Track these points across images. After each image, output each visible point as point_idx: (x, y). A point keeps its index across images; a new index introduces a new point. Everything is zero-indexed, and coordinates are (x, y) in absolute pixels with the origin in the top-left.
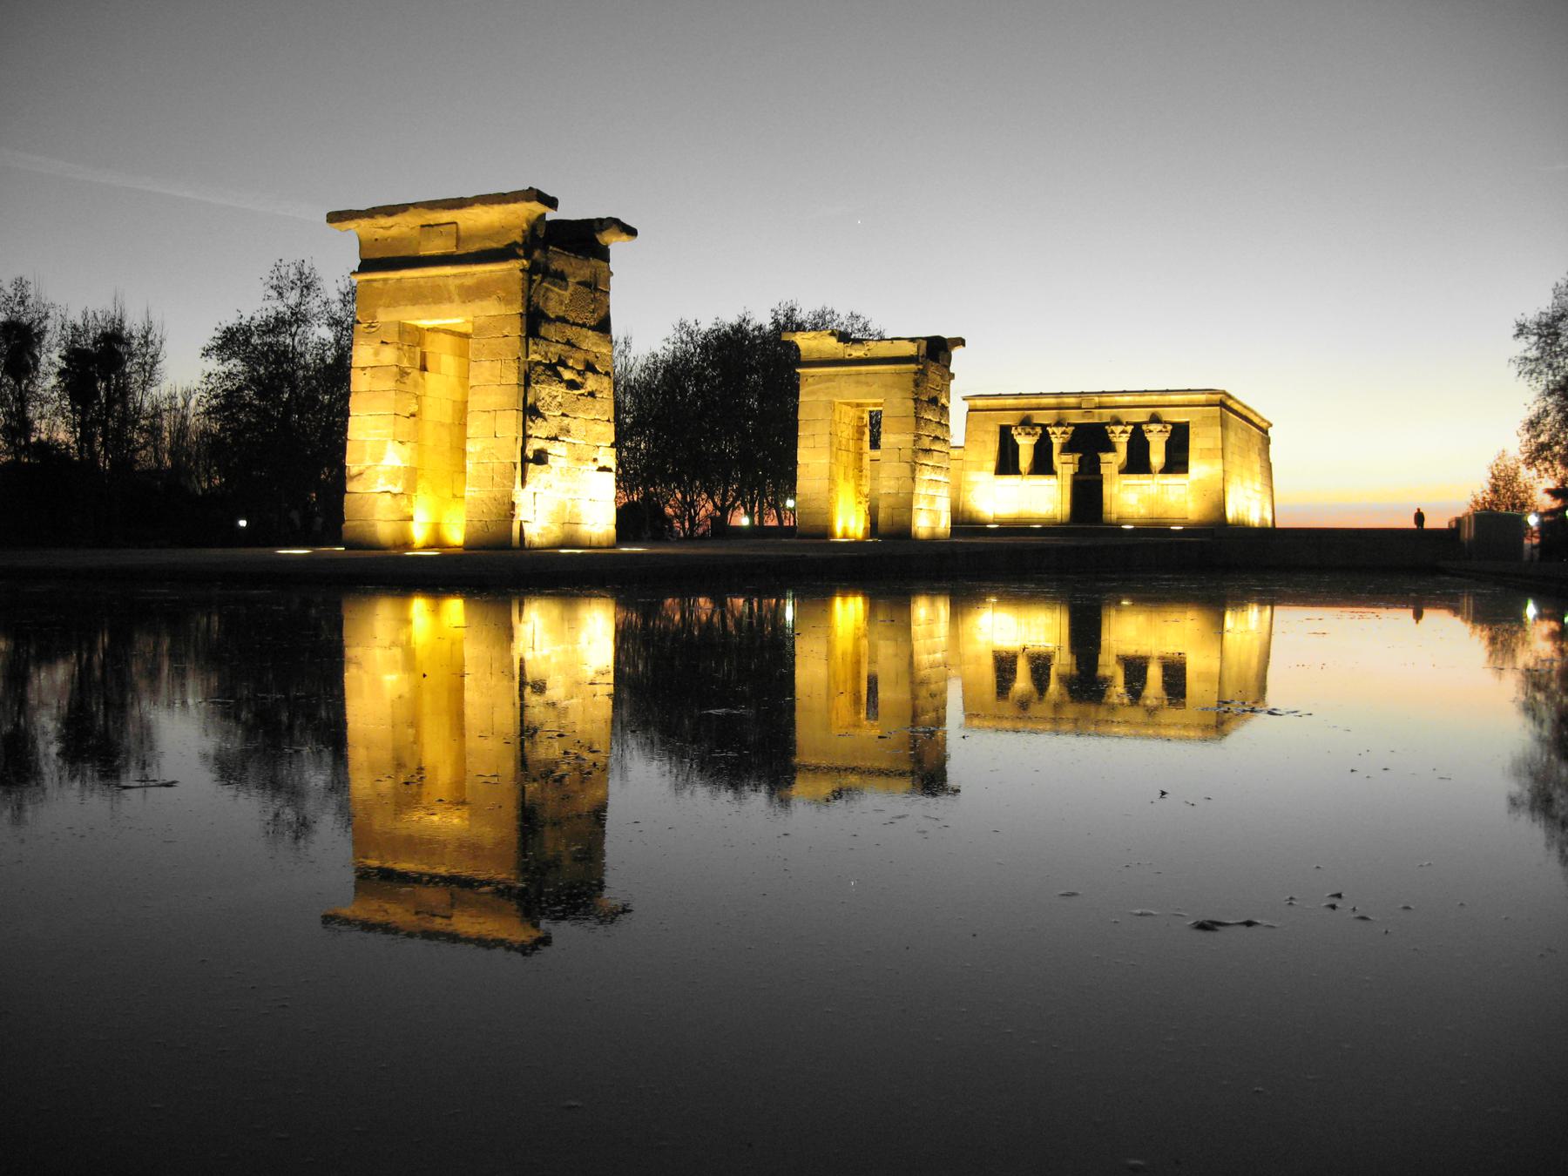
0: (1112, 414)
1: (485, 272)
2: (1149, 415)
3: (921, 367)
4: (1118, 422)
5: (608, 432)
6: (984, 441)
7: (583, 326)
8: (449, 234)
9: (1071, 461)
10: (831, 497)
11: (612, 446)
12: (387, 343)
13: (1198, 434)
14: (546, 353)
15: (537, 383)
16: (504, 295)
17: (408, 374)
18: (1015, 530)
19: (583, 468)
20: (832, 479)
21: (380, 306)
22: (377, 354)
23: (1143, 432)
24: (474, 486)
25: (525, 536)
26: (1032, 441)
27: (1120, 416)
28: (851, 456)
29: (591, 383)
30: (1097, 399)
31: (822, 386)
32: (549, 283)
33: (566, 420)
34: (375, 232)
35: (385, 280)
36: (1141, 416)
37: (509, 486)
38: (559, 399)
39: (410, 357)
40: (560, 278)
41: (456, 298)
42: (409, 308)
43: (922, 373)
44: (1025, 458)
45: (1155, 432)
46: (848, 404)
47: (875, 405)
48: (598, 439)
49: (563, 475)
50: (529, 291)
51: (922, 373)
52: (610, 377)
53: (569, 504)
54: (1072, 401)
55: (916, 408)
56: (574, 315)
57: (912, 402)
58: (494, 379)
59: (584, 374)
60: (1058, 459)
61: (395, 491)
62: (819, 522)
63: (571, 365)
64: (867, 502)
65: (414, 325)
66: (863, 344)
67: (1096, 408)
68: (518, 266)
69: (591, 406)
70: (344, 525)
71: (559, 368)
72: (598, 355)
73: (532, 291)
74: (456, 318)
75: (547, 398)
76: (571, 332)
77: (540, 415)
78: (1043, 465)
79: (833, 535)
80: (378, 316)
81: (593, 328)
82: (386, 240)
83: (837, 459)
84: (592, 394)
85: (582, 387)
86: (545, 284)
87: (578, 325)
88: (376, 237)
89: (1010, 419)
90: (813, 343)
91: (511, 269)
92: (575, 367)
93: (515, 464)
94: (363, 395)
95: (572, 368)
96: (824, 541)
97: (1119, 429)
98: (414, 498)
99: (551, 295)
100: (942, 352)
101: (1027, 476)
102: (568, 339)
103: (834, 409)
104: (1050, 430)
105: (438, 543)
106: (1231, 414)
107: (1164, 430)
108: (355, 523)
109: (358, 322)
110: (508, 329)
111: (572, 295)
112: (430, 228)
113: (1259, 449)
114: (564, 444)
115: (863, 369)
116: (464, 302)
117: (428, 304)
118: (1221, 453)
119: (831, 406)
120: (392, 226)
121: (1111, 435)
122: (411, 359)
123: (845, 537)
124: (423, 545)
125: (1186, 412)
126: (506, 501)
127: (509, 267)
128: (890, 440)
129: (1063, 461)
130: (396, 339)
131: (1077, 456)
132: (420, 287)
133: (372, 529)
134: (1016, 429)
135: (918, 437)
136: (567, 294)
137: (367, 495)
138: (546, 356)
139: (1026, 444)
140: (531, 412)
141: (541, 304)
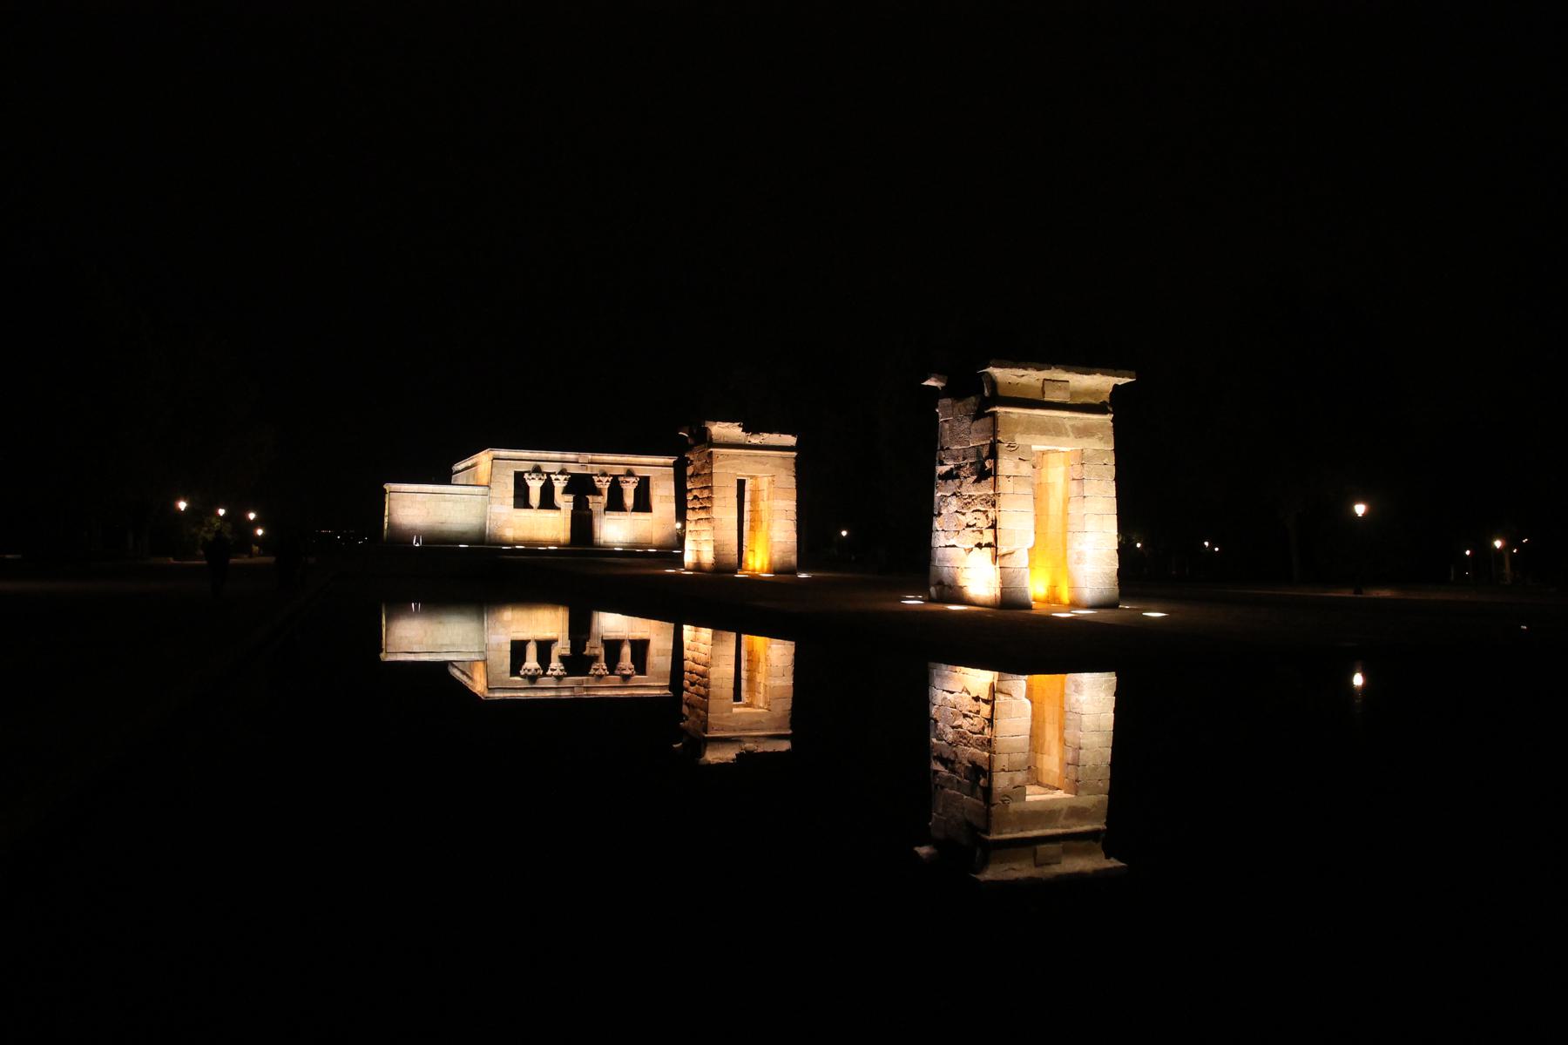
1: (1089, 419)
4: (604, 475)
6: (506, 483)
22: (1017, 466)
26: (541, 483)
27: (606, 470)
30: (590, 457)
35: (1018, 413)
36: (620, 470)
44: (535, 497)
67: (589, 463)
74: (1068, 446)
78: (547, 502)
89: (524, 467)
94: (1010, 496)
97: (606, 479)
104: (553, 477)
116: (1076, 438)
117: (1052, 435)
120: (1023, 376)
132: (1046, 423)
134: (530, 475)
139: (535, 485)
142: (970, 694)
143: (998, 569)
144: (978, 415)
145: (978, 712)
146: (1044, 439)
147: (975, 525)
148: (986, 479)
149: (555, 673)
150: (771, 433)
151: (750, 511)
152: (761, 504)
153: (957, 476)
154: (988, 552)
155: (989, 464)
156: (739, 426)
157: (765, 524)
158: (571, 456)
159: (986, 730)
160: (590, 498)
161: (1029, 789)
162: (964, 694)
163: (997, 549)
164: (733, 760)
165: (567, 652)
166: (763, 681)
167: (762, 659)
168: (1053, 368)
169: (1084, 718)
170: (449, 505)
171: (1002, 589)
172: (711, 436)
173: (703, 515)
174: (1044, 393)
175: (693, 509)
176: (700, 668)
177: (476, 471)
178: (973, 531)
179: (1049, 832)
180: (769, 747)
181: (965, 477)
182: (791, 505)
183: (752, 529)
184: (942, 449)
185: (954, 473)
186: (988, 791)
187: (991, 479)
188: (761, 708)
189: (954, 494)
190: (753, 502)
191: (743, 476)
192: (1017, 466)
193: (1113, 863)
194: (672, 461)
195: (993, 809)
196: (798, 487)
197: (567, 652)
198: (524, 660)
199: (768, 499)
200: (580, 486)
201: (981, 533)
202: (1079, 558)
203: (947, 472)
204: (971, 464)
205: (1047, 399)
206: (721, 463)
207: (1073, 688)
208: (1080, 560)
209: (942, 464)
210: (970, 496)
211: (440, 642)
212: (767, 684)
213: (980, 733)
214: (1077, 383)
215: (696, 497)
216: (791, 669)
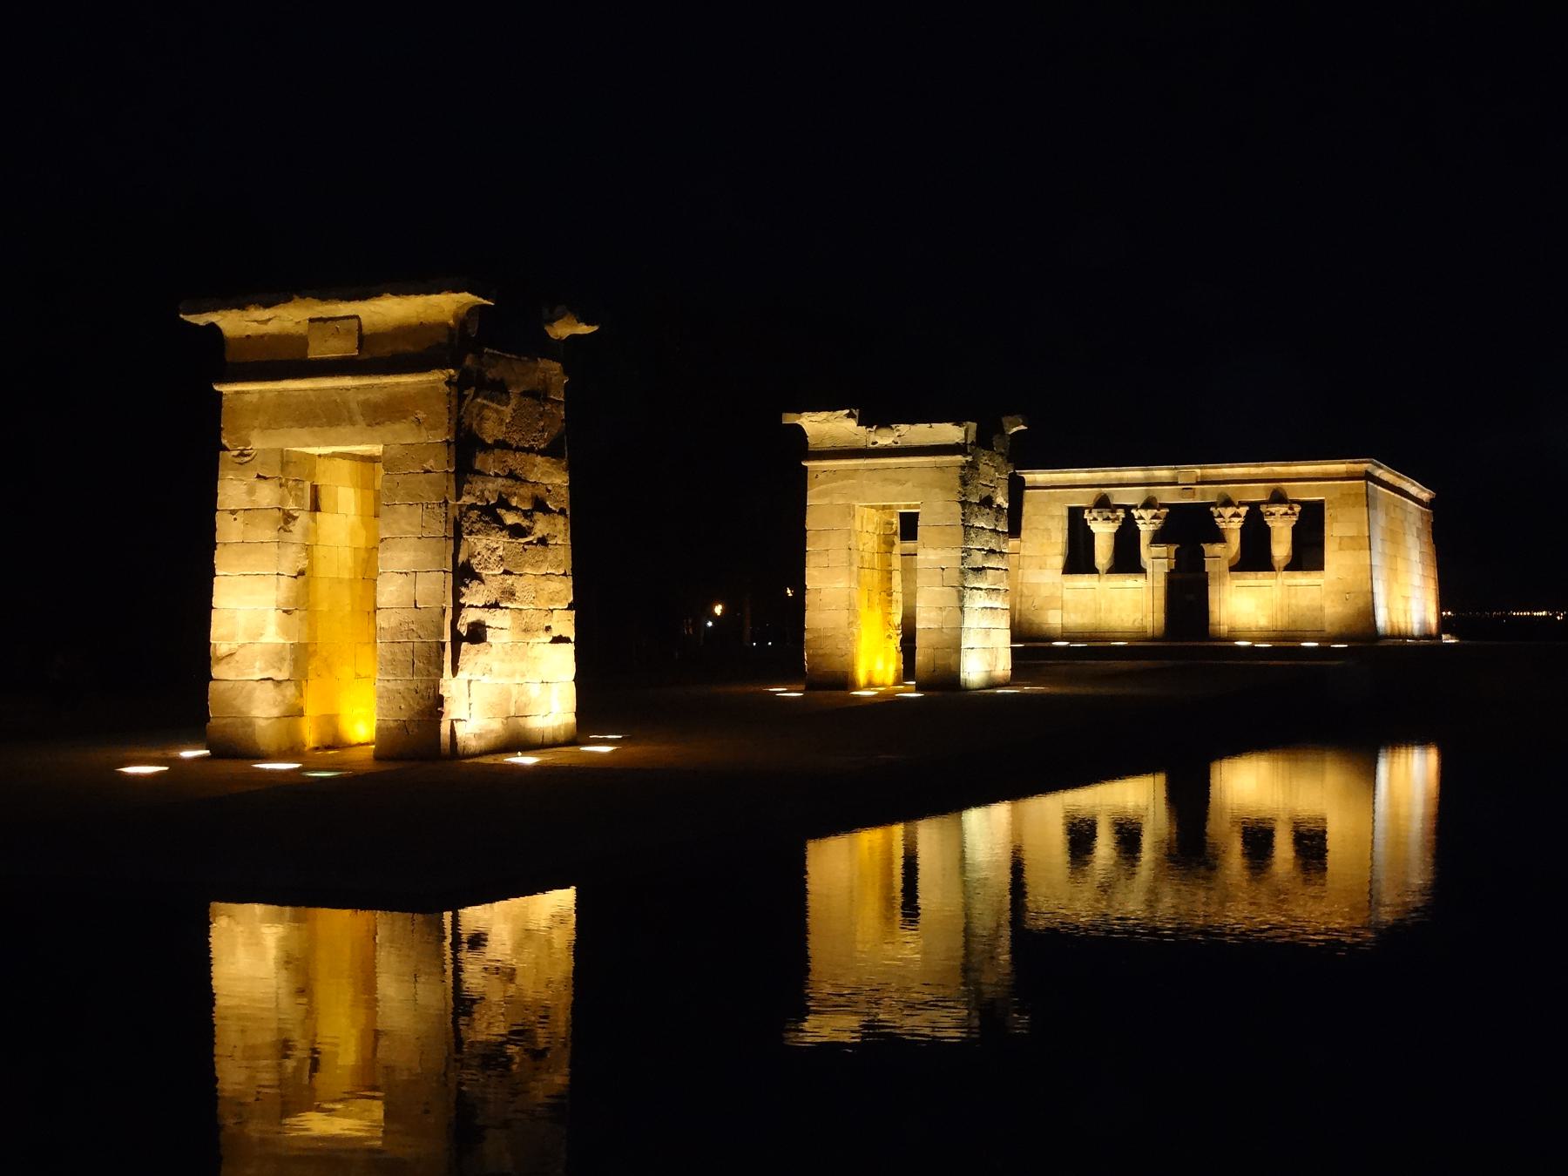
0: (1220, 491)
2: (1270, 493)
3: (969, 458)
4: (1228, 503)
5: (564, 589)
6: (1047, 530)
7: (530, 450)
8: (349, 332)
9: (1165, 555)
10: (853, 634)
11: (570, 607)
12: (265, 478)
13: (1337, 518)
14: (482, 492)
15: (471, 533)
16: (424, 416)
17: (295, 518)
19: (531, 641)
20: (851, 609)
21: (255, 427)
22: (251, 491)
23: (1261, 515)
24: (387, 673)
25: (458, 740)
27: (1230, 496)
28: (877, 576)
29: (541, 527)
30: (1198, 471)
31: (840, 483)
32: (485, 398)
33: (510, 580)
34: (247, 326)
35: (260, 391)
36: (1258, 493)
37: (436, 675)
38: (500, 552)
39: (296, 495)
40: (498, 390)
41: (359, 418)
42: (296, 431)
43: (972, 466)
44: (1103, 552)
45: (1278, 515)
46: (872, 507)
47: (908, 507)
48: (551, 600)
49: (506, 653)
50: (460, 405)
51: (972, 466)
52: (566, 516)
53: (515, 691)
55: (964, 514)
56: (517, 437)
57: (959, 507)
58: (414, 530)
59: (532, 515)
60: (1147, 553)
61: (280, 677)
62: (836, 665)
63: (514, 504)
64: (898, 635)
65: (301, 452)
66: (892, 429)
67: (1198, 483)
68: (442, 377)
69: (542, 558)
70: (208, 724)
71: (498, 511)
72: (550, 488)
73: (462, 413)
75: (484, 552)
76: (514, 460)
77: (477, 577)
78: (1126, 560)
79: (855, 686)
80: (252, 442)
81: (542, 453)
82: (262, 337)
83: (859, 582)
84: (543, 541)
85: (530, 534)
86: (479, 400)
87: (519, 449)
88: (249, 333)
89: (1083, 498)
90: (826, 427)
91: (435, 381)
92: (520, 506)
93: (443, 645)
95: (516, 509)
96: (841, 693)
97: (1229, 511)
98: (304, 683)
99: (487, 413)
100: (998, 436)
101: (1106, 576)
102: (510, 470)
103: (854, 516)
104: (1136, 513)
105: (335, 743)
106: (1379, 488)
107: (1290, 512)
108: (224, 721)
109: (226, 449)
110: (431, 462)
111: (514, 411)
112: (322, 323)
113: (1418, 528)
114: (508, 611)
116: (369, 425)
118: (1367, 540)
119: (849, 512)
120: (270, 320)
121: (1218, 520)
122: (298, 499)
123: (870, 685)
124: (316, 746)
125: (1319, 488)
126: (431, 695)
127: (431, 378)
128: (932, 557)
129: (1154, 555)
130: (278, 473)
131: (1174, 548)
133: (250, 730)
134: (1090, 512)
135: (968, 551)
136: (508, 410)
137: (241, 684)
138: (482, 497)
139: (1103, 532)
140: (464, 574)
141: (474, 426)
146: (304, 433)
150: (912, 422)
156: (850, 416)
158: (1163, 473)
168: (296, 297)
174: (307, 345)
192: (251, 491)
205: (312, 355)
214: (376, 318)
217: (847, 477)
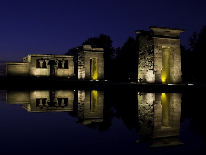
4: (57, 60)
6: (35, 62)
18: (41, 78)
22: (158, 51)
36: (61, 59)
42: (163, 44)
44: (41, 66)
54: (50, 56)
78: (44, 67)
89: (39, 58)
90: (87, 47)
97: (58, 61)
104: (45, 61)
109: (154, 45)
115: (95, 52)
125: (68, 59)
139: (41, 62)
142: (148, 104)
143: (154, 75)
144: (149, 39)
145: (150, 108)
146: (165, 45)
147: (149, 65)
148: (151, 54)
149: (46, 106)
150: (98, 47)
151: (93, 66)
152: (96, 64)
153: (144, 54)
154: (152, 70)
155: (152, 51)
156: (91, 46)
157: (96, 69)
158: (50, 56)
159: (152, 112)
160: (54, 65)
161: (162, 126)
162: (146, 104)
163: (154, 70)
164: (90, 124)
165: (49, 101)
166: (97, 105)
167: (96, 100)
169: (174, 109)
170: (22, 67)
171: (155, 79)
172: (84, 49)
173: (82, 67)
174: (164, 34)
175: (80, 66)
176: (82, 102)
177: (27, 60)
178: (148, 66)
179: (167, 136)
180: (98, 121)
181: (146, 54)
182: (102, 64)
183: (93, 70)
184: (140, 48)
185: (144, 53)
186: (153, 127)
187: (153, 54)
188: (96, 112)
189: (144, 58)
190: (94, 64)
191: (91, 58)
193: (181, 143)
194: (73, 57)
195: (154, 131)
196: (104, 60)
197: (49, 101)
198: (39, 104)
199: (97, 63)
200: (52, 63)
201: (150, 66)
202: (173, 72)
203: (142, 53)
204: (148, 51)
205: (165, 35)
206: (87, 55)
207: (172, 102)
208: (173, 72)
209: (140, 51)
210: (147, 58)
211: (20, 99)
212: (98, 106)
213: (151, 113)
214: (172, 32)
215: (80, 63)
216: (103, 103)
217: (89, 54)
